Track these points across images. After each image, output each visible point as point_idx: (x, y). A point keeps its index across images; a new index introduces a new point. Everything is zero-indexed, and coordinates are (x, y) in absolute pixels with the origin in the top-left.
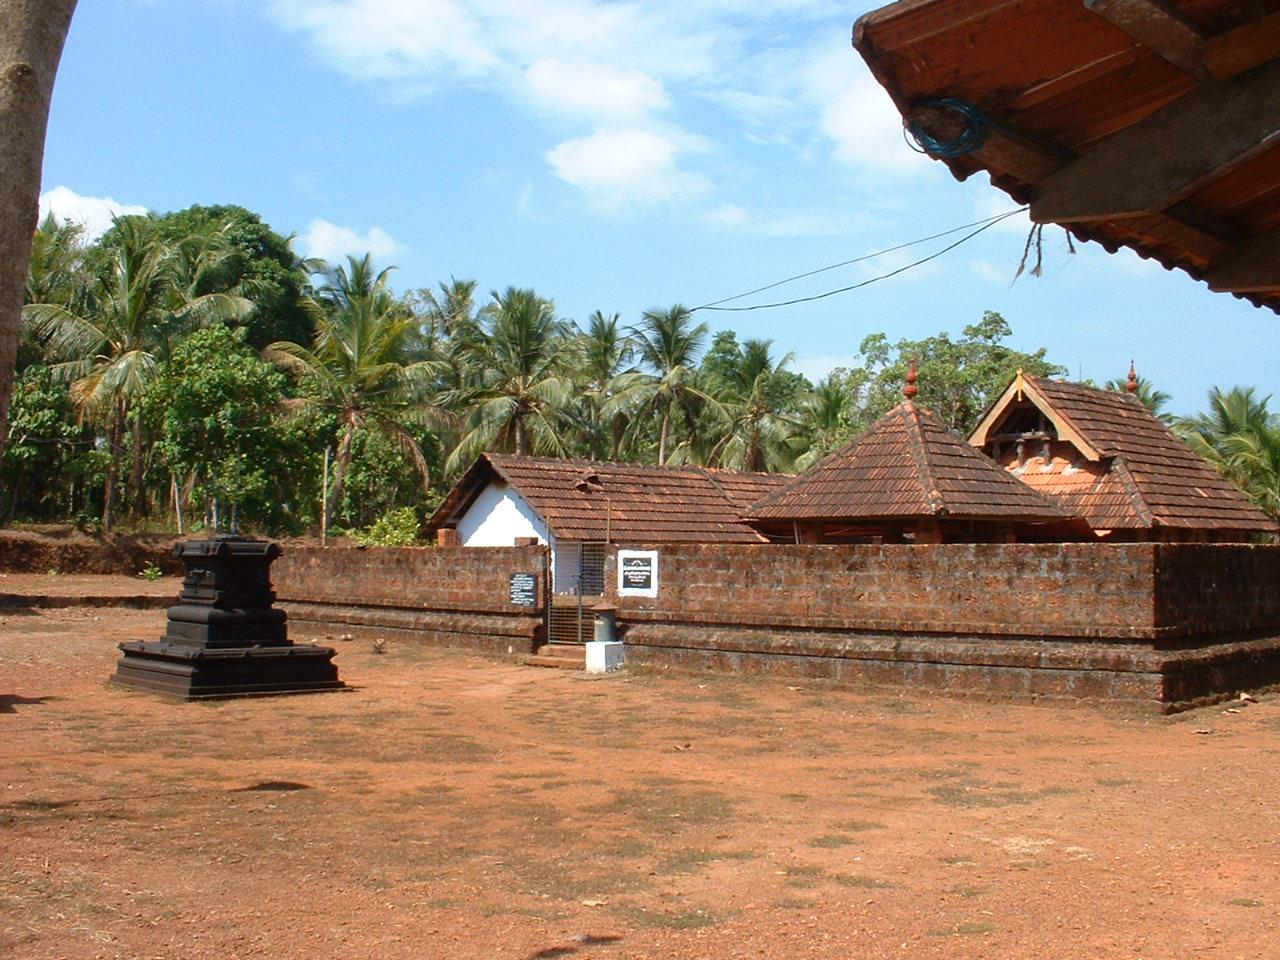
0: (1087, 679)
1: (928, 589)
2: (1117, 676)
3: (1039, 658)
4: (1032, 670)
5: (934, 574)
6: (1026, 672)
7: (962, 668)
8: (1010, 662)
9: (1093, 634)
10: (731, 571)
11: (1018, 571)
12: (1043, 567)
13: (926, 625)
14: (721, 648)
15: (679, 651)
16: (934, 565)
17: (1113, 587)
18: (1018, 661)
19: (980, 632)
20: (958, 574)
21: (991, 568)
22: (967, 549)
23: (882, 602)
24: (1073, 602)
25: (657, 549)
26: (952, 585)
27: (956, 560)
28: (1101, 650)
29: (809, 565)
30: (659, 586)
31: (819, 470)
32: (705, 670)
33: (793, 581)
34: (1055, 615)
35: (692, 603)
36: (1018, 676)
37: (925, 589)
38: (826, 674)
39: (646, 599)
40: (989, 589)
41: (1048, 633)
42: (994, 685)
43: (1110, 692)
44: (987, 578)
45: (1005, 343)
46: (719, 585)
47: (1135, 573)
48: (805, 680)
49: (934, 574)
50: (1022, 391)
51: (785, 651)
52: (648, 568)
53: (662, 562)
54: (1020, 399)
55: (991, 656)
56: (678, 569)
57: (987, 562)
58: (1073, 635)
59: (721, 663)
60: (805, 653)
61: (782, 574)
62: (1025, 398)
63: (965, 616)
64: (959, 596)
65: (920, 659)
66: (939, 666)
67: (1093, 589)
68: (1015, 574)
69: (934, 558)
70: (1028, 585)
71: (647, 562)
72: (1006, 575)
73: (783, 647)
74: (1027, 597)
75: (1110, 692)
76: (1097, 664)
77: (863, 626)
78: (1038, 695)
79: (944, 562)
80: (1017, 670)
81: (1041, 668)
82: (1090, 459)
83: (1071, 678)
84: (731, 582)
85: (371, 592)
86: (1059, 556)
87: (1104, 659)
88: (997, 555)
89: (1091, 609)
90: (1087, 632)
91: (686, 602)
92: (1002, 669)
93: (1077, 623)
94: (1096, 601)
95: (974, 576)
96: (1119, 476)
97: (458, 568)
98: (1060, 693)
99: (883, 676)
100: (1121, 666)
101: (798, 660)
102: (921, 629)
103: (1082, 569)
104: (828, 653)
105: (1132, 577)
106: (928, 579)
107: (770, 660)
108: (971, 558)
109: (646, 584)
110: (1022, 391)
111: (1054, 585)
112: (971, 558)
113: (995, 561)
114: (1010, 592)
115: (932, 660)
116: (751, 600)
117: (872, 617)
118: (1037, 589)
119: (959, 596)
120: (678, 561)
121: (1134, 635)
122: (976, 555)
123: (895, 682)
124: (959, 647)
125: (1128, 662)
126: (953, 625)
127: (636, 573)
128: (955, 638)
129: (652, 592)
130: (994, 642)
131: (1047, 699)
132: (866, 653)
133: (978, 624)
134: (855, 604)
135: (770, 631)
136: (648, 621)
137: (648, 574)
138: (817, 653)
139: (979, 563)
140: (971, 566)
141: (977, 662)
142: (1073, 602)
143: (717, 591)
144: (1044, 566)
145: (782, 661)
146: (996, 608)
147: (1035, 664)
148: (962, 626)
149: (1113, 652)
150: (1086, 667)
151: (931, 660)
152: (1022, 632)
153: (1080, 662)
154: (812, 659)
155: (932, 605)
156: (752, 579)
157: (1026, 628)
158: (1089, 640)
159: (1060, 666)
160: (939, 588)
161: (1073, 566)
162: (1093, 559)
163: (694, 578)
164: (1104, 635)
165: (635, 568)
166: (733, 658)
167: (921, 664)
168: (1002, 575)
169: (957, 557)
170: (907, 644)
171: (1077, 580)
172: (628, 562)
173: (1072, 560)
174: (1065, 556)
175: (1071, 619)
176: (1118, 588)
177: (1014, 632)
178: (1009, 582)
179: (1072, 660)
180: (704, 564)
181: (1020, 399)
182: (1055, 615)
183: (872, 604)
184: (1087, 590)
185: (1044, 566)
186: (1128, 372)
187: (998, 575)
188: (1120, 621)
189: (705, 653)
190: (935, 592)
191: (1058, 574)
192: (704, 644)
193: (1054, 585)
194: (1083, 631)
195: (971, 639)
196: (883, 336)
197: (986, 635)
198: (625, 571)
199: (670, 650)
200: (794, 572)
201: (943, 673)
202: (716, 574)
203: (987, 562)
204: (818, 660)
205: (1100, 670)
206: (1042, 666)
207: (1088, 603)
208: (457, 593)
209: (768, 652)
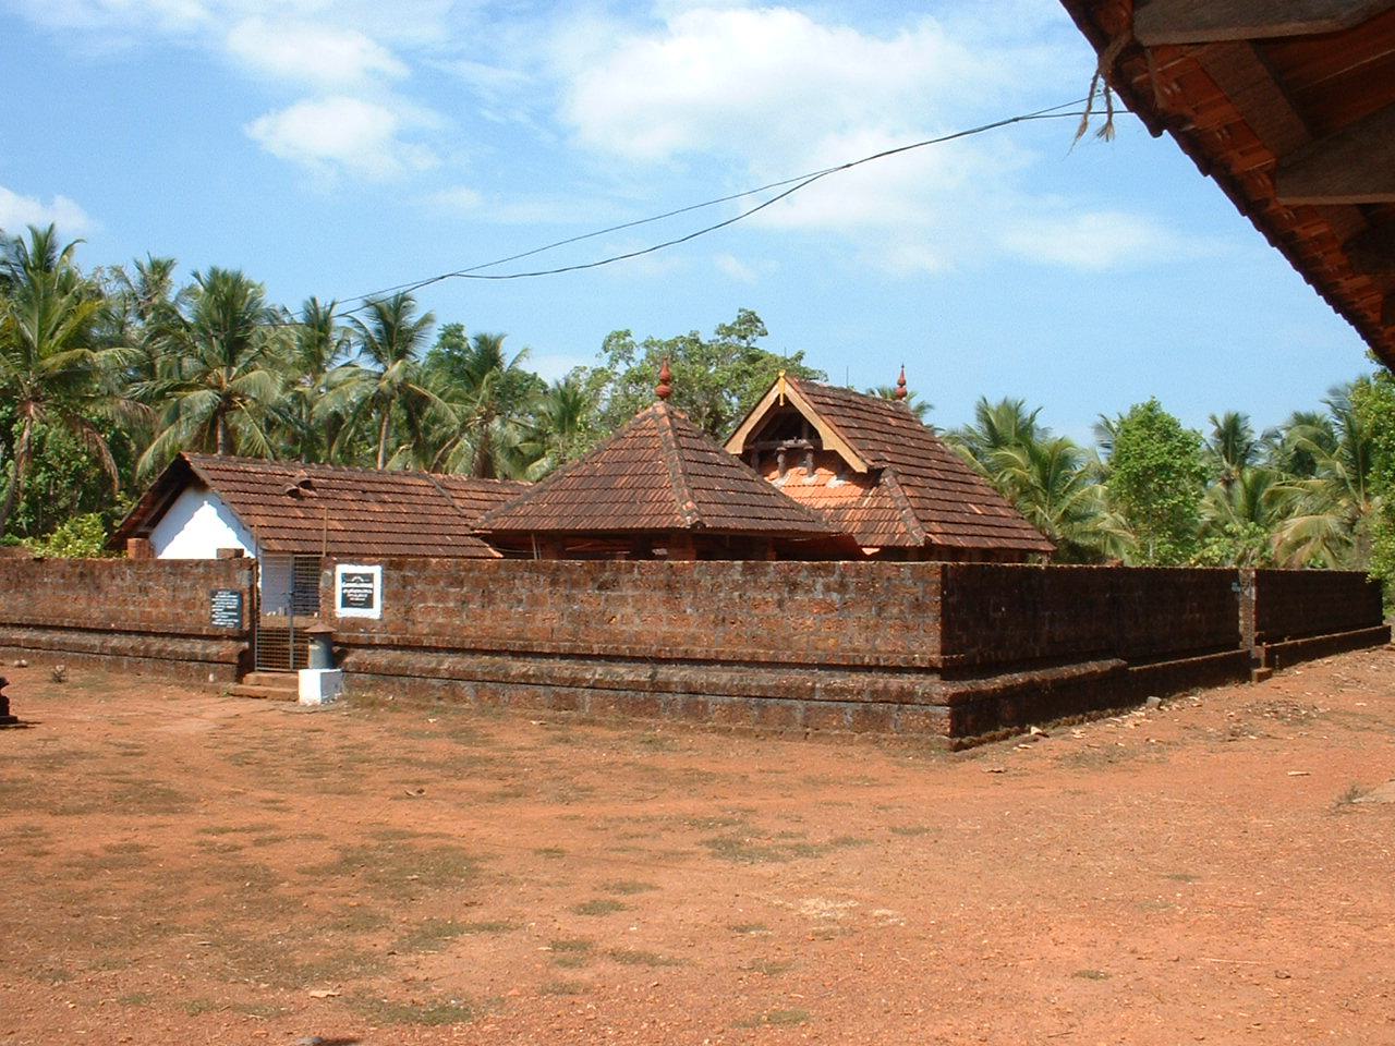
1: (689, 611)
2: (899, 709)
3: (813, 689)
5: (696, 594)
6: (799, 704)
7: (727, 699)
9: (873, 663)
10: (465, 589)
11: (790, 592)
12: (817, 587)
13: (686, 652)
14: (454, 677)
15: (405, 680)
16: (695, 584)
17: (895, 611)
18: (788, 693)
19: (747, 659)
20: (722, 595)
21: (760, 588)
22: (733, 566)
23: (636, 626)
24: (852, 627)
25: (380, 563)
26: (716, 607)
27: (720, 579)
28: (882, 681)
29: (554, 583)
30: (382, 605)
31: (561, 478)
32: (434, 702)
33: (535, 601)
34: (831, 642)
35: (421, 625)
36: (790, 708)
37: (685, 612)
38: (573, 706)
39: (367, 621)
40: (757, 612)
41: (823, 661)
42: (763, 719)
43: (892, 726)
44: (754, 599)
45: (761, 344)
46: (452, 604)
47: (920, 595)
48: (549, 713)
49: (696, 594)
50: (784, 395)
51: (526, 680)
52: (369, 585)
53: (386, 579)
54: (782, 404)
55: (760, 687)
56: (404, 587)
57: (756, 582)
58: (851, 663)
59: (454, 693)
60: (549, 682)
61: (524, 594)
62: (786, 398)
63: (729, 642)
64: (724, 620)
65: (679, 690)
66: (701, 698)
67: (873, 613)
68: (786, 595)
69: (696, 576)
70: (800, 608)
71: (369, 578)
72: (776, 597)
73: (524, 675)
74: (800, 621)
75: (892, 726)
76: (880, 696)
77: (615, 652)
78: (812, 729)
79: (707, 581)
80: (789, 702)
81: (815, 700)
82: (858, 471)
84: (464, 602)
85: (50, 610)
86: (835, 576)
87: (886, 690)
88: (766, 574)
89: (870, 634)
91: (414, 624)
92: (772, 700)
93: (855, 650)
94: (876, 626)
95: (740, 596)
96: (888, 489)
97: (151, 583)
98: (836, 728)
99: (637, 708)
100: (904, 698)
101: (541, 690)
102: (680, 656)
103: (862, 590)
104: (574, 682)
105: (917, 600)
106: (689, 600)
107: (510, 691)
108: (737, 577)
109: (368, 603)
110: (784, 395)
111: (830, 608)
112: (737, 577)
113: (764, 580)
114: (781, 615)
115: (692, 690)
116: (488, 623)
117: (625, 642)
118: (811, 612)
119: (724, 620)
120: (404, 577)
121: (918, 663)
122: (743, 574)
123: (651, 715)
124: (723, 676)
125: (912, 694)
126: (717, 652)
127: (355, 591)
128: (718, 666)
129: (374, 613)
130: (763, 671)
131: (821, 735)
132: (618, 683)
133: (745, 651)
134: (606, 627)
135: (510, 658)
136: (370, 646)
137: (370, 592)
138: (563, 682)
140: (737, 586)
141: (744, 692)
142: (852, 627)
143: (448, 612)
144: (819, 587)
145: (523, 692)
147: (809, 694)
149: (895, 683)
150: (866, 700)
151: (691, 691)
152: (794, 659)
153: (858, 693)
154: (557, 689)
155: (692, 630)
156: (489, 599)
157: (798, 656)
158: (868, 668)
159: (837, 698)
160: (701, 610)
161: (852, 588)
162: (874, 579)
163: (423, 597)
164: (886, 663)
165: (355, 585)
166: (467, 688)
170: (664, 672)
171: (855, 603)
172: (347, 577)
173: (851, 580)
174: (843, 576)
175: (848, 646)
176: (901, 611)
177: (785, 659)
178: (780, 603)
179: (850, 691)
180: (434, 581)
181: (782, 404)
182: (831, 642)
183: (624, 628)
184: (867, 614)
185: (819, 587)
186: (898, 377)
187: (768, 596)
188: (903, 648)
189: (434, 682)
190: (695, 614)
191: (835, 596)
192: (434, 673)
193: (830, 608)
194: (862, 658)
195: (736, 667)
196: (627, 334)
197: (754, 663)
198: (343, 589)
199: (395, 679)
200: (536, 591)
201: (705, 705)
202: (447, 593)
203: (756, 582)
204: (565, 691)
205: (882, 702)
206: (817, 697)
207: (868, 627)
208: (150, 612)
209: (508, 680)
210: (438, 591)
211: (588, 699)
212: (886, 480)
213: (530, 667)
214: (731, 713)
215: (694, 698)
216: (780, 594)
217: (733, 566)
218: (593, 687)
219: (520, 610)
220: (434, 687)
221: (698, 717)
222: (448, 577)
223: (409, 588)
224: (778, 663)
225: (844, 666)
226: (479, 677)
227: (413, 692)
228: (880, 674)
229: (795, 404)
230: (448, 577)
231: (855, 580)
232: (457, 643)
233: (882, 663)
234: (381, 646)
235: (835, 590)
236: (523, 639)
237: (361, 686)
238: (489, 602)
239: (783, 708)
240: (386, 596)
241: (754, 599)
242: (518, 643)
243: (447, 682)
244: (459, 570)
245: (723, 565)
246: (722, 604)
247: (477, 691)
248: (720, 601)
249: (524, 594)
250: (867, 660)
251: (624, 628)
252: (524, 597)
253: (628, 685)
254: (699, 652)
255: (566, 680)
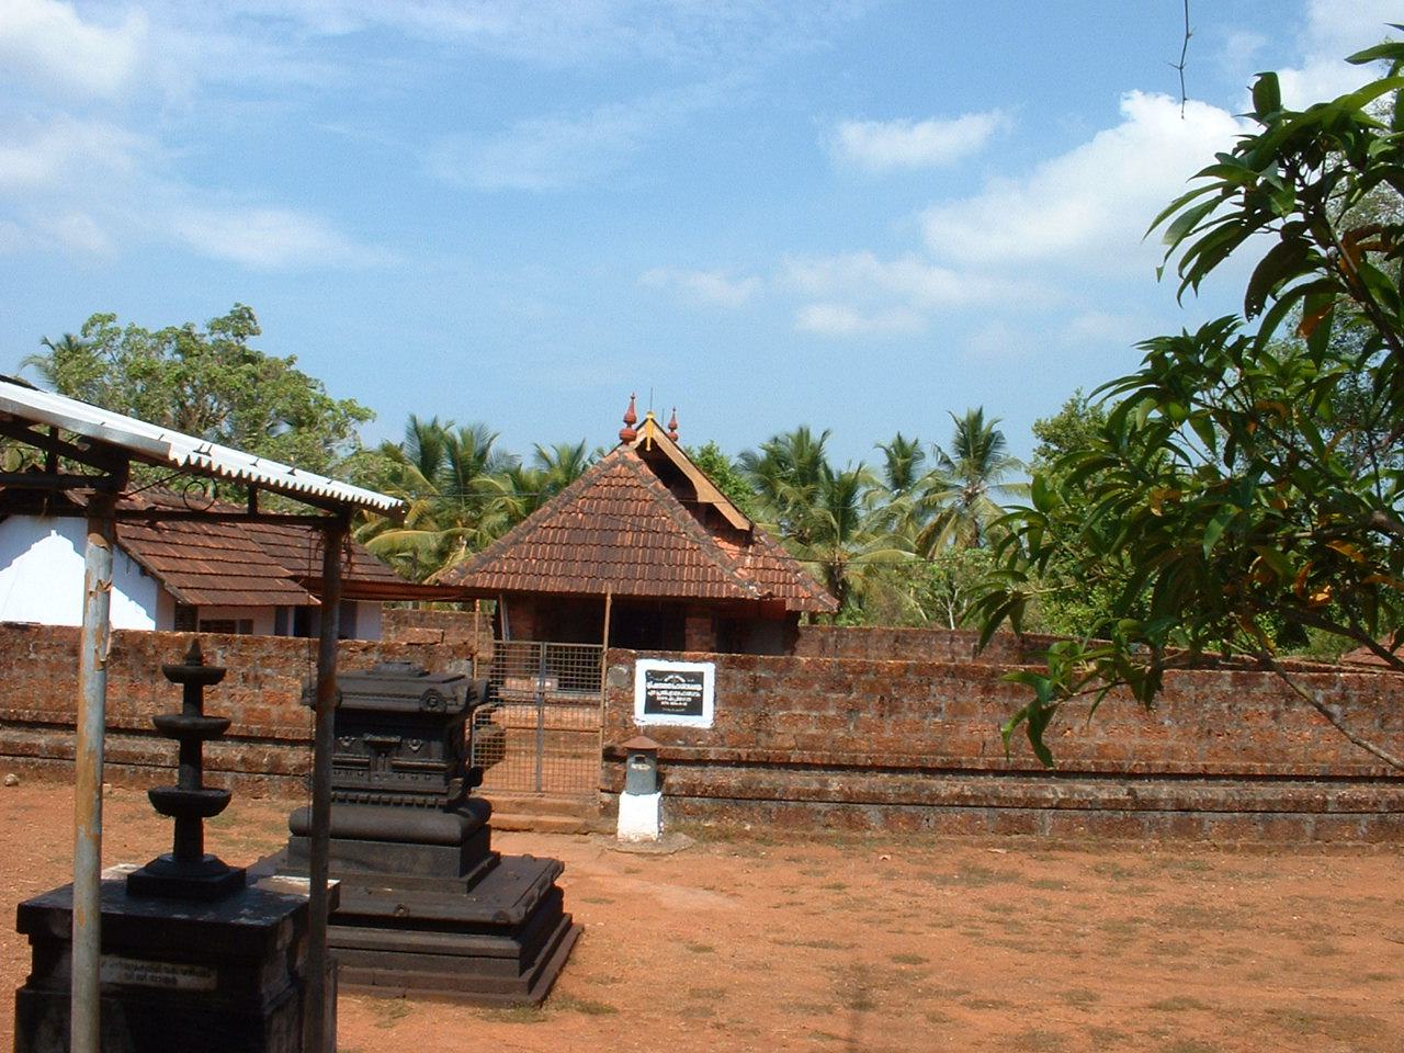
0: (1382, 823)
1: (1167, 722)
3: (1326, 802)
4: (1316, 815)
5: (1176, 705)
6: (1310, 818)
8: (1289, 807)
9: (1380, 773)
10: (854, 695)
11: (1287, 703)
13: (1168, 766)
14: (850, 800)
15: (773, 806)
16: (1175, 695)
18: (1299, 806)
19: (1240, 773)
21: (1253, 699)
22: (1221, 676)
23: (1100, 737)
25: (714, 660)
26: (1200, 718)
27: (1207, 690)
29: (987, 690)
30: (716, 712)
31: (535, 528)
32: (818, 830)
33: (960, 711)
34: (1331, 753)
35: (780, 738)
36: (1296, 823)
38: (1030, 829)
39: (691, 731)
40: (1249, 724)
41: (1326, 773)
42: (1269, 833)
45: (251, 344)
46: (832, 713)
48: (999, 838)
50: (652, 439)
51: (962, 801)
52: (698, 687)
53: (721, 679)
54: (648, 449)
55: (1266, 802)
56: (754, 691)
57: (1248, 693)
59: (849, 819)
60: (995, 804)
61: (943, 701)
62: (653, 442)
63: (1216, 754)
64: (1209, 732)
65: (1168, 807)
66: (1195, 815)
67: (1377, 725)
68: (1282, 707)
69: (1176, 686)
71: (698, 678)
73: (959, 796)
74: (1297, 733)
77: (1076, 768)
78: (1325, 840)
79: (1190, 691)
80: (1297, 816)
82: (738, 527)
83: (1364, 823)
84: (854, 710)
85: (42, 702)
88: (1260, 685)
90: (1373, 771)
91: (769, 734)
92: (1279, 814)
93: (1356, 762)
95: (1230, 707)
96: (769, 549)
97: (268, 671)
99: (1112, 829)
101: (985, 812)
103: (1364, 701)
104: (1032, 803)
107: (934, 815)
108: (1227, 688)
109: (695, 707)
110: (652, 439)
112: (1227, 688)
114: (1276, 727)
115: (1185, 807)
116: (889, 734)
117: (1084, 756)
118: (1310, 724)
119: (1209, 732)
120: (754, 679)
122: (1233, 684)
123: (1133, 835)
124: (1218, 791)
126: (1205, 766)
127: (676, 693)
128: (1202, 781)
129: (704, 721)
130: (1253, 784)
131: (1337, 847)
132: (1090, 802)
133: (1238, 764)
134: (1059, 740)
135: (920, 775)
136: (701, 762)
137: (698, 695)
138: (1016, 803)
139: (1235, 693)
140: (1225, 697)
141: (1247, 808)
143: (823, 721)
145: (957, 815)
146: (1257, 746)
148: (1216, 765)
150: (1382, 810)
151: (1181, 807)
152: (1294, 772)
153: (1375, 804)
154: (1006, 811)
155: (1171, 742)
156: (889, 706)
158: (1370, 779)
161: (1355, 700)
162: (1377, 691)
163: (785, 703)
164: (1393, 774)
165: (669, 686)
166: (873, 814)
167: (1170, 813)
168: (1266, 708)
169: (1207, 686)
170: (1144, 789)
171: (1358, 715)
172: (653, 676)
173: (1353, 693)
174: (1344, 688)
177: (1285, 772)
178: (1275, 716)
179: (1366, 803)
180: (805, 683)
181: (648, 449)
182: (1331, 753)
183: (1083, 741)
186: (625, 411)
189: (820, 806)
192: (821, 795)
194: (1369, 769)
196: (111, 318)
197: (1251, 777)
198: (648, 690)
199: (753, 803)
200: (961, 699)
201: (1200, 823)
202: (825, 699)
203: (1248, 693)
204: (1016, 813)
208: (266, 712)
209: (934, 802)
210: (810, 696)
211: (1049, 820)
212: (762, 538)
213: (963, 786)
214: (1231, 831)
215: (1186, 816)
216: (1276, 705)
217: (1221, 676)
218: (1057, 808)
219: (937, 720)
220: (819, 812)
221: (1192, 836)
222: (826, 680)
223: (762, 692)
224: (1276, 776)
225: (1348, 777)
226: (892, 799)
227: (785, 819)
228: (1382, 784)
229: (666, 451)
230: (826, 680)
231: (1357, 692)
232: (844, 758)
233: (1389, 774)
234: (717, 763)
235: (1336, 703)
236: (942, 754)
237: (699, 813)
238: (891, 712)
239: (1291, 822)
240: (723, 700)
241: (1246, 710)
242: (939, 758)
243: (840, 806)
244: (845, 672)
245: (1210, 675)
246: (1208, 716)
247: (886, 816)
248: (1206, 712)
249: (943, 701)
250: (1373, 771)
251: (1083, 741)
252: (943, 705)
253: (1104, 803)
254: (1183, 766)
255: (1018, 800)
